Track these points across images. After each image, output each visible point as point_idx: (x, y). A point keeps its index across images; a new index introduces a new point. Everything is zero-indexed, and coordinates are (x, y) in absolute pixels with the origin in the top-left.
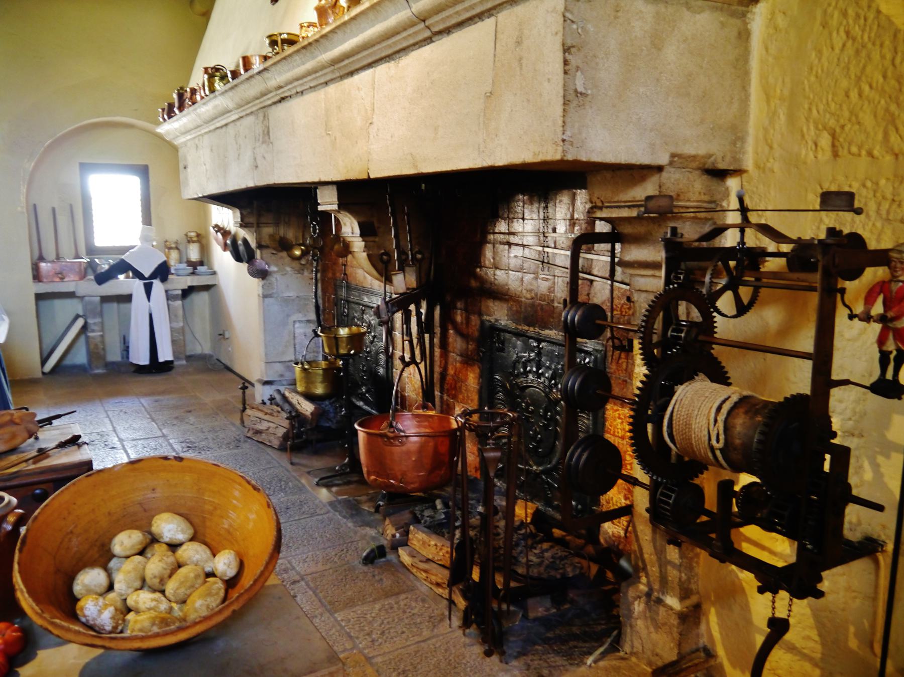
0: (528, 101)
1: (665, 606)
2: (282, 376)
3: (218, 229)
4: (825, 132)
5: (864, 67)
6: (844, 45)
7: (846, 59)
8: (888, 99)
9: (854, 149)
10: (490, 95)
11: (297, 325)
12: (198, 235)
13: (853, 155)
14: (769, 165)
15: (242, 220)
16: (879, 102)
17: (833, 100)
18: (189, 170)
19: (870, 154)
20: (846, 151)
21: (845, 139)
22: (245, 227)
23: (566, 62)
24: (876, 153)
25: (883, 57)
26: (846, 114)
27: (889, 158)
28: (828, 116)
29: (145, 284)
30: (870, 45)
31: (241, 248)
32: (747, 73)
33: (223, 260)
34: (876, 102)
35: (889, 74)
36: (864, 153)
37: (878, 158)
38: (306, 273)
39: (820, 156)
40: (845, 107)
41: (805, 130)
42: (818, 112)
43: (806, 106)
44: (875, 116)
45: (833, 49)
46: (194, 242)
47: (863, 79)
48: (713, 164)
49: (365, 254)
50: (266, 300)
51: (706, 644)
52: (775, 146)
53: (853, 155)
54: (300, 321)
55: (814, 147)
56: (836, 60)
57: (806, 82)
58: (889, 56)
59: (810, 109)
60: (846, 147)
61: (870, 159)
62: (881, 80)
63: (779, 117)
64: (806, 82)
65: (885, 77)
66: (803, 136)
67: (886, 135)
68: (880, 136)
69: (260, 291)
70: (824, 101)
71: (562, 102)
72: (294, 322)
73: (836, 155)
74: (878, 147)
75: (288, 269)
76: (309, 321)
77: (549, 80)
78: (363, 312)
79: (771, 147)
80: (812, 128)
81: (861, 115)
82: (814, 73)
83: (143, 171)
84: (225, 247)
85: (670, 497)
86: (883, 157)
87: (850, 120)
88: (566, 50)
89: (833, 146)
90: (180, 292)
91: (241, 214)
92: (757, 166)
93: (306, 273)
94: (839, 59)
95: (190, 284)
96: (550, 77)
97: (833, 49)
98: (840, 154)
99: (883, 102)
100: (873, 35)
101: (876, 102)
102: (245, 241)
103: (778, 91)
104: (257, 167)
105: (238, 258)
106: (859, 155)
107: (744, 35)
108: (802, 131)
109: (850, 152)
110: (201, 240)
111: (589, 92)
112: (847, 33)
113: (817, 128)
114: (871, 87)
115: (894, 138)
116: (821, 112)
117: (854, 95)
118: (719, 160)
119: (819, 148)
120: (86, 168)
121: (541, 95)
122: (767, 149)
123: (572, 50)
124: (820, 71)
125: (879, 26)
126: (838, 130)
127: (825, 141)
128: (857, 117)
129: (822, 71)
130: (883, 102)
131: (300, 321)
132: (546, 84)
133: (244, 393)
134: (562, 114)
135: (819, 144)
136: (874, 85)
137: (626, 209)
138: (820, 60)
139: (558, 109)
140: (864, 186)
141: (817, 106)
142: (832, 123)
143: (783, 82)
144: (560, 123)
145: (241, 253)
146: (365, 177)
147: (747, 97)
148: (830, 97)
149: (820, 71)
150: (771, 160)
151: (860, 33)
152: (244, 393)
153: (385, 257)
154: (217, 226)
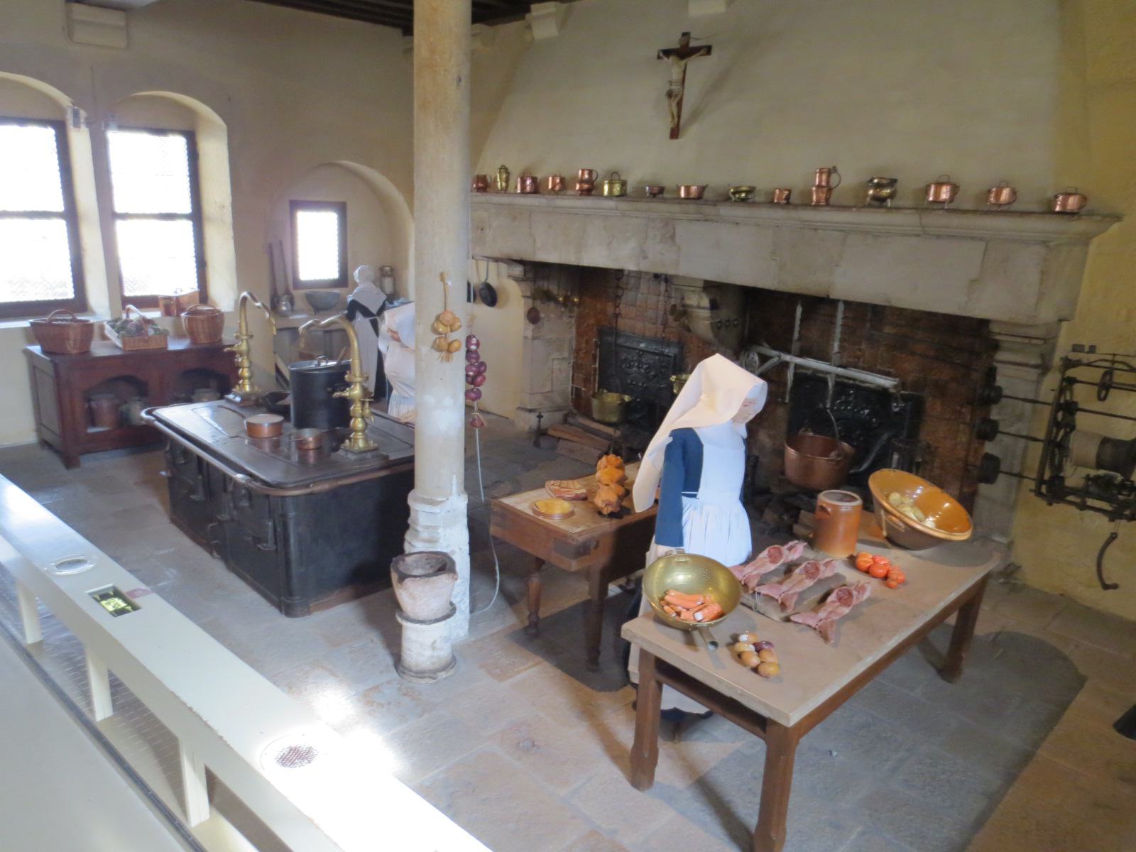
10: (973, 281)
11: (555, 362)
12: (392, 270)
22: (526, 281)
29: (371, 321)
38: (565, 319)
46: (389, 276)
49: (708, 322)
50: (536, 342)
54: (558, 359)
69: (529, 334)
72: (553, 360)
75: (552, 315)
76: (563, 359)
78: (640, 356)
88: (1043, 273)
93: (565, 319)
104: (645, 258)
107: (1086, 253)
120: (296, 205)
131: (558, 359)
133: (539, 421)
146: (823, 295)
152: (539, 421)
153: (719, 324)
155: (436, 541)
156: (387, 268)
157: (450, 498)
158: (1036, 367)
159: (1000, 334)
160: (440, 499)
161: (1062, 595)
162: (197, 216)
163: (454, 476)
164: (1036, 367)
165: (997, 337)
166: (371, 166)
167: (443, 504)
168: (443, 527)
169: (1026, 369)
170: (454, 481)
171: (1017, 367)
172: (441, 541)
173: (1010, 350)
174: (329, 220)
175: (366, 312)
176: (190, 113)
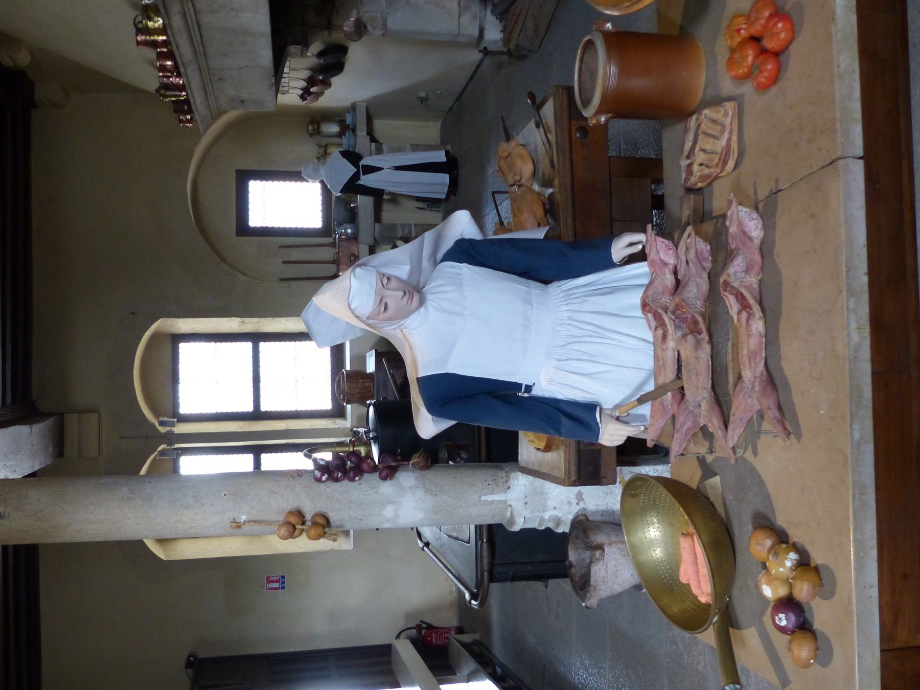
2: (475, 17)
3: (306, 94)
15: (298, 43)
18: (245, 96)
31: (329, 60)
33: (341, 92)
46: (319, 127)
83: (243, 177)
84: (327, 84)
90: (373, 144)
91: (293, 44)
95: (365, 133)
102: (320, 55)
105: (337, 67)
110: (317, 119)
120: (243, 229)
145: (332, 64)
154: (302, 97)
155: (559, 519)
156: (310, 128)
157: (509, 503)
160: (509, 514)
162: (256, 338)
163: (483, 498)
166: (191, 154)
167: (516, 514)
168: (544, 511)
170: (490, 498)
172: (560, 515)
174: (255, 187)
175: (356, 177)
176: (155, 337)
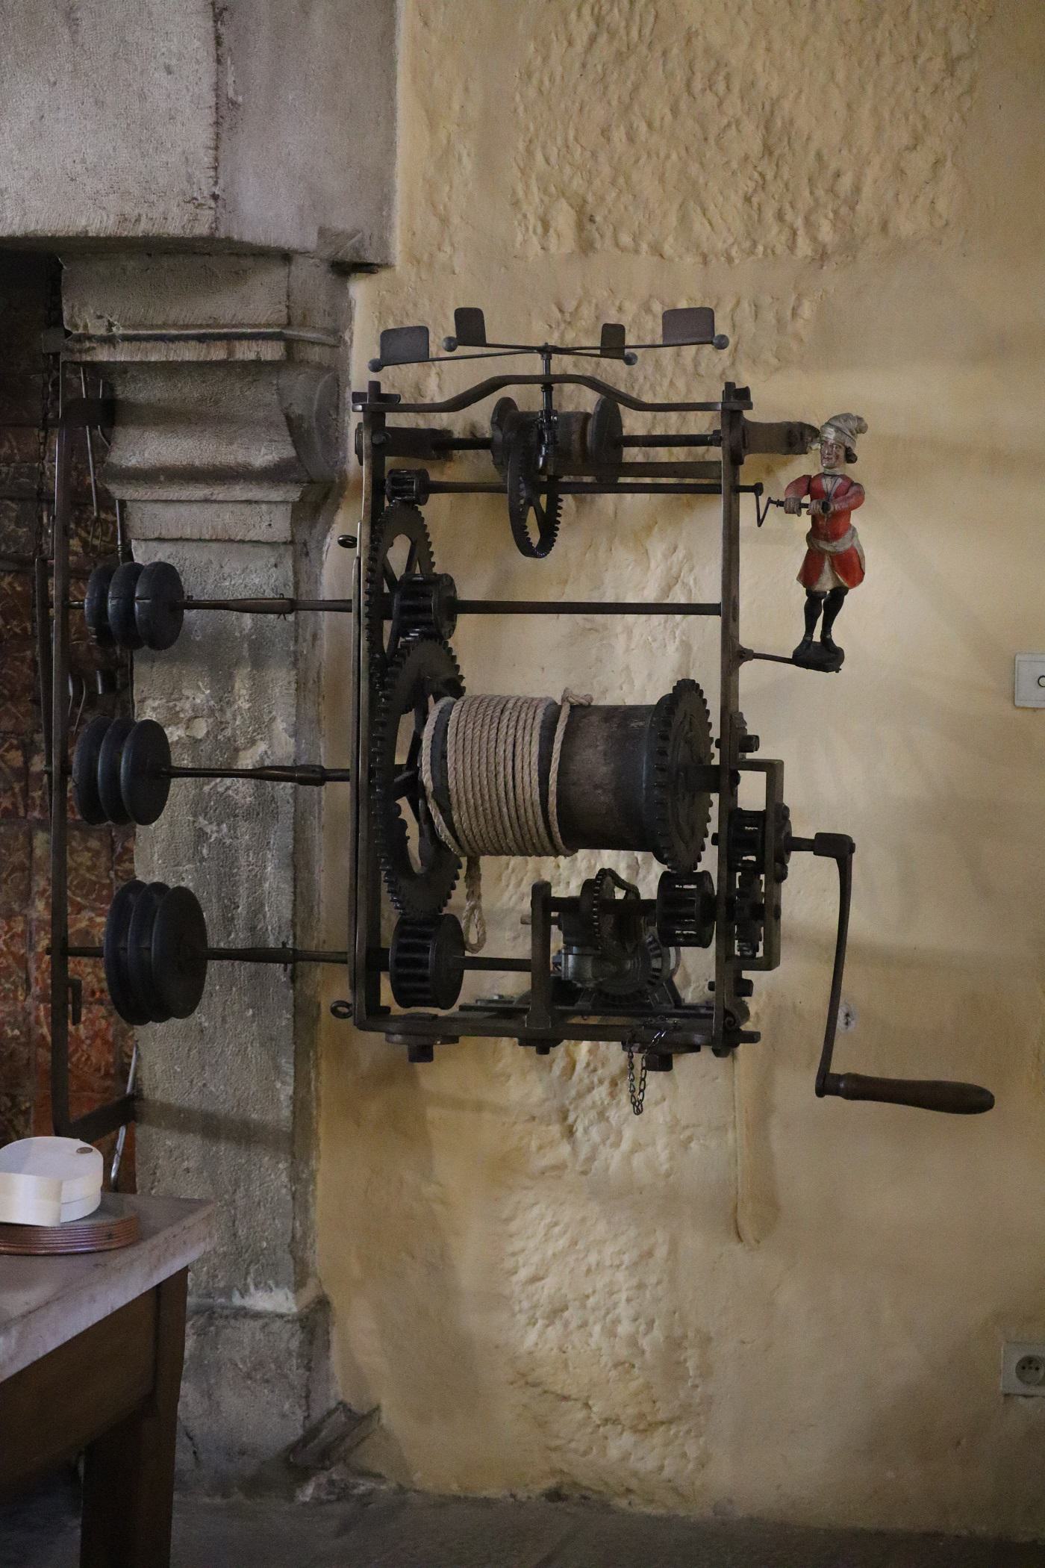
0: (99, 104)
1: (257, 1315)
4: (563, 200)
5: (636, 88)
6: (593, 39)
7: (599, 68)
8: (683, 153)
9: (626, 239)
13: (623, 250)
14: (442, 257)
16: (668, 157)
17: (576, 139)
19: (657, 250)
20: (608, 241)
21: (605, 218)
23: (218, 41)
24: (668, 249)
25: (669, 76)
26: (606, 170)
27: (690, 260)
28: (568, 170)
30: (643, 49)
32: (392, 62)
34: (662, 155)
35: (683, 106)
36: (644, 247)
37: (671, 260)
39: (553, 248)
40: (602, 158)
41: (521, 194)
42: (547, 161)
43: (521, 146)
44: (662, 180)
45: (570, 43)
47: (636, 108)
48: (357, 250)
51: (341, 1397)
52: (455, 220)
53: (623, 250)
55: (540, 230)
56: (577, 65)
57: (518, 98)
58: (680, 75)
59: (530, 152)
60: (609, 234)
61: (656, 258)
62: (669, 117)
63: (460, 160)
64: (518, 98)
65: (675, 111)
66: (516, 204)
67: (684, 219)
68: (673, 219)
70: (559, 141)
71: (211, 120)
73: (586, 247)
74: (671, 239)
77: (169, 70)
79: (445, 221)
80: (535, 189)
81: (635, 177)
82: (535, 81)
85: (426, 950)
86: (681, 257)
87: (613, 183)
89: (580, 227)
92: (414, 259)
94: (584, 65)
96: (174, 62)
97: (570, 43)
98: (598, 245)
99: (674, 156)
100: (647, 31)
101: (662, 155)
103: (456, 107)
106: (637, 251)
108: (514, 193)
109: (617, 245)
111: (240, 99)
112: (598, 20)
113: (545, 191)
114: (650, 125)
115: (699, 225)
116: (553, 160)
117: (619, 135)
118: (367, 243)
119: (552, 231)
121: (142, 97)
122: (434, 224)
123: (226, 15)
124: (547, 82)
125: (656, 17)
126: (590, 198)
127: (564, 218)
128: (628, 179)
129: (552, 79)
130: (674, 156)
132: (160, 76)
134: (212, 144)
135: (553, 223)
136: (657, 124)
137: (193, 343)
138: (546, 59)
139: (200, 134)
140: (648, 310)
141: (544, 147)
142: (577, 183)
143: (467, 90)
144: (207, 160)
147: (393, 112)
148: (571, 134)
149: (547, 82)
150: (448, 249)
151: (623, 24)
158: (274, 475)
159: (109, 340)
161: (555, 1495)
164: (274, 475)
165: (103, 355)
169: (239, 492)
171: (199, 492)
173: (167, 418)
